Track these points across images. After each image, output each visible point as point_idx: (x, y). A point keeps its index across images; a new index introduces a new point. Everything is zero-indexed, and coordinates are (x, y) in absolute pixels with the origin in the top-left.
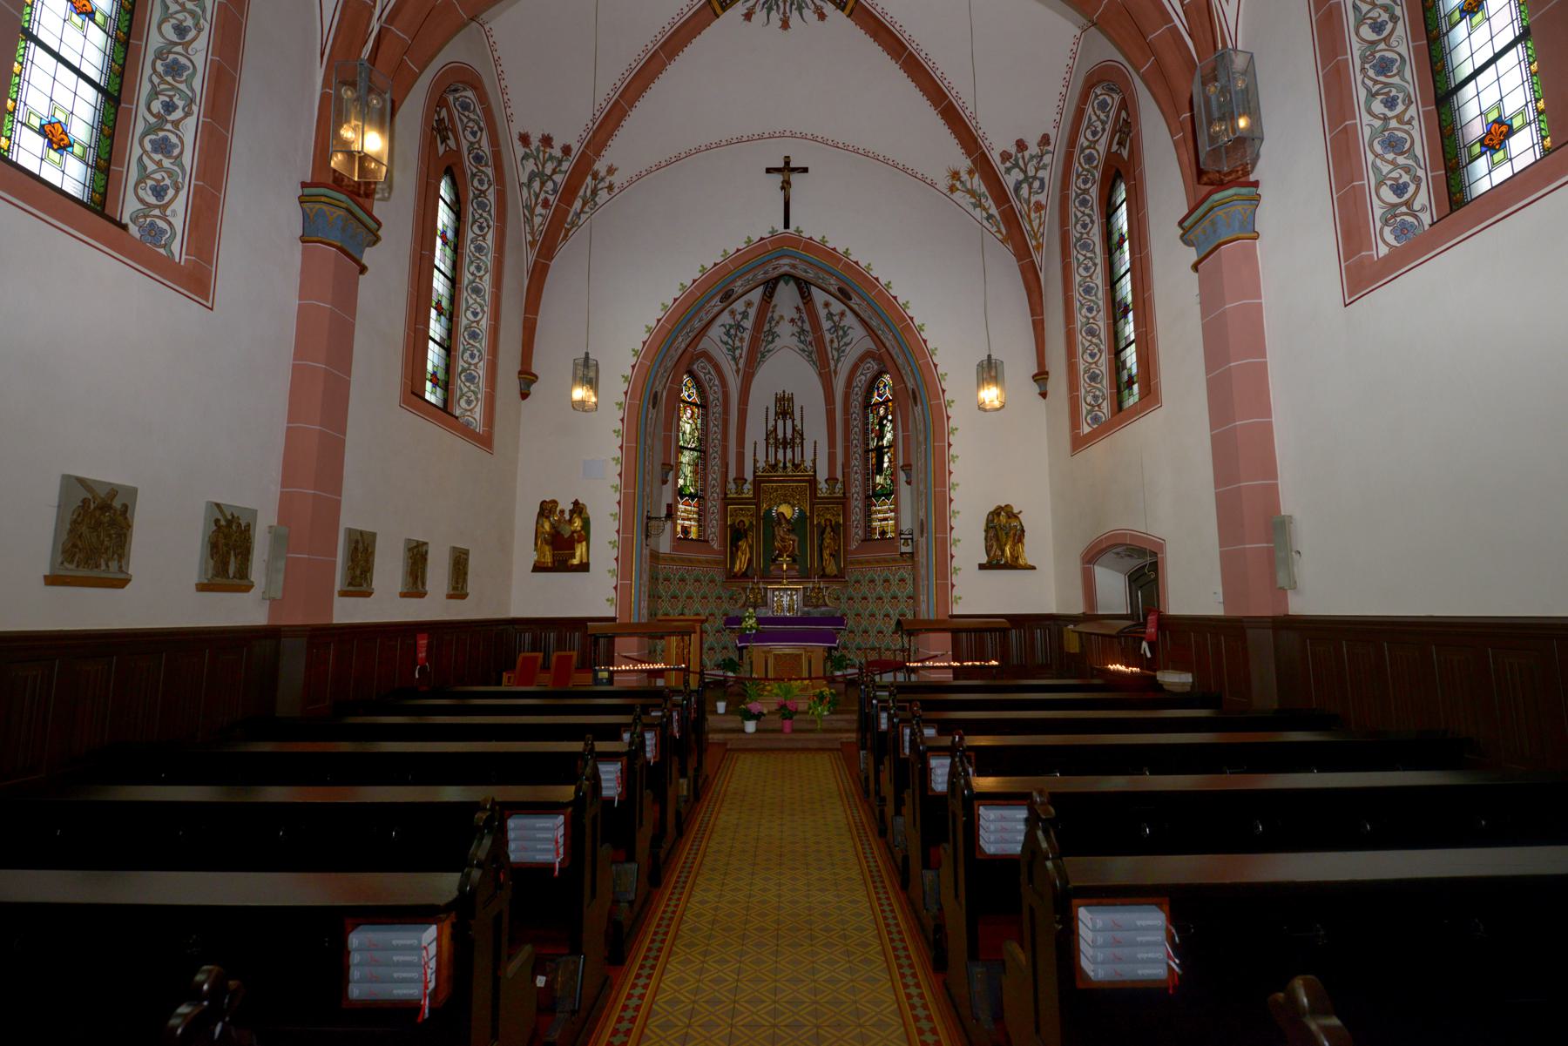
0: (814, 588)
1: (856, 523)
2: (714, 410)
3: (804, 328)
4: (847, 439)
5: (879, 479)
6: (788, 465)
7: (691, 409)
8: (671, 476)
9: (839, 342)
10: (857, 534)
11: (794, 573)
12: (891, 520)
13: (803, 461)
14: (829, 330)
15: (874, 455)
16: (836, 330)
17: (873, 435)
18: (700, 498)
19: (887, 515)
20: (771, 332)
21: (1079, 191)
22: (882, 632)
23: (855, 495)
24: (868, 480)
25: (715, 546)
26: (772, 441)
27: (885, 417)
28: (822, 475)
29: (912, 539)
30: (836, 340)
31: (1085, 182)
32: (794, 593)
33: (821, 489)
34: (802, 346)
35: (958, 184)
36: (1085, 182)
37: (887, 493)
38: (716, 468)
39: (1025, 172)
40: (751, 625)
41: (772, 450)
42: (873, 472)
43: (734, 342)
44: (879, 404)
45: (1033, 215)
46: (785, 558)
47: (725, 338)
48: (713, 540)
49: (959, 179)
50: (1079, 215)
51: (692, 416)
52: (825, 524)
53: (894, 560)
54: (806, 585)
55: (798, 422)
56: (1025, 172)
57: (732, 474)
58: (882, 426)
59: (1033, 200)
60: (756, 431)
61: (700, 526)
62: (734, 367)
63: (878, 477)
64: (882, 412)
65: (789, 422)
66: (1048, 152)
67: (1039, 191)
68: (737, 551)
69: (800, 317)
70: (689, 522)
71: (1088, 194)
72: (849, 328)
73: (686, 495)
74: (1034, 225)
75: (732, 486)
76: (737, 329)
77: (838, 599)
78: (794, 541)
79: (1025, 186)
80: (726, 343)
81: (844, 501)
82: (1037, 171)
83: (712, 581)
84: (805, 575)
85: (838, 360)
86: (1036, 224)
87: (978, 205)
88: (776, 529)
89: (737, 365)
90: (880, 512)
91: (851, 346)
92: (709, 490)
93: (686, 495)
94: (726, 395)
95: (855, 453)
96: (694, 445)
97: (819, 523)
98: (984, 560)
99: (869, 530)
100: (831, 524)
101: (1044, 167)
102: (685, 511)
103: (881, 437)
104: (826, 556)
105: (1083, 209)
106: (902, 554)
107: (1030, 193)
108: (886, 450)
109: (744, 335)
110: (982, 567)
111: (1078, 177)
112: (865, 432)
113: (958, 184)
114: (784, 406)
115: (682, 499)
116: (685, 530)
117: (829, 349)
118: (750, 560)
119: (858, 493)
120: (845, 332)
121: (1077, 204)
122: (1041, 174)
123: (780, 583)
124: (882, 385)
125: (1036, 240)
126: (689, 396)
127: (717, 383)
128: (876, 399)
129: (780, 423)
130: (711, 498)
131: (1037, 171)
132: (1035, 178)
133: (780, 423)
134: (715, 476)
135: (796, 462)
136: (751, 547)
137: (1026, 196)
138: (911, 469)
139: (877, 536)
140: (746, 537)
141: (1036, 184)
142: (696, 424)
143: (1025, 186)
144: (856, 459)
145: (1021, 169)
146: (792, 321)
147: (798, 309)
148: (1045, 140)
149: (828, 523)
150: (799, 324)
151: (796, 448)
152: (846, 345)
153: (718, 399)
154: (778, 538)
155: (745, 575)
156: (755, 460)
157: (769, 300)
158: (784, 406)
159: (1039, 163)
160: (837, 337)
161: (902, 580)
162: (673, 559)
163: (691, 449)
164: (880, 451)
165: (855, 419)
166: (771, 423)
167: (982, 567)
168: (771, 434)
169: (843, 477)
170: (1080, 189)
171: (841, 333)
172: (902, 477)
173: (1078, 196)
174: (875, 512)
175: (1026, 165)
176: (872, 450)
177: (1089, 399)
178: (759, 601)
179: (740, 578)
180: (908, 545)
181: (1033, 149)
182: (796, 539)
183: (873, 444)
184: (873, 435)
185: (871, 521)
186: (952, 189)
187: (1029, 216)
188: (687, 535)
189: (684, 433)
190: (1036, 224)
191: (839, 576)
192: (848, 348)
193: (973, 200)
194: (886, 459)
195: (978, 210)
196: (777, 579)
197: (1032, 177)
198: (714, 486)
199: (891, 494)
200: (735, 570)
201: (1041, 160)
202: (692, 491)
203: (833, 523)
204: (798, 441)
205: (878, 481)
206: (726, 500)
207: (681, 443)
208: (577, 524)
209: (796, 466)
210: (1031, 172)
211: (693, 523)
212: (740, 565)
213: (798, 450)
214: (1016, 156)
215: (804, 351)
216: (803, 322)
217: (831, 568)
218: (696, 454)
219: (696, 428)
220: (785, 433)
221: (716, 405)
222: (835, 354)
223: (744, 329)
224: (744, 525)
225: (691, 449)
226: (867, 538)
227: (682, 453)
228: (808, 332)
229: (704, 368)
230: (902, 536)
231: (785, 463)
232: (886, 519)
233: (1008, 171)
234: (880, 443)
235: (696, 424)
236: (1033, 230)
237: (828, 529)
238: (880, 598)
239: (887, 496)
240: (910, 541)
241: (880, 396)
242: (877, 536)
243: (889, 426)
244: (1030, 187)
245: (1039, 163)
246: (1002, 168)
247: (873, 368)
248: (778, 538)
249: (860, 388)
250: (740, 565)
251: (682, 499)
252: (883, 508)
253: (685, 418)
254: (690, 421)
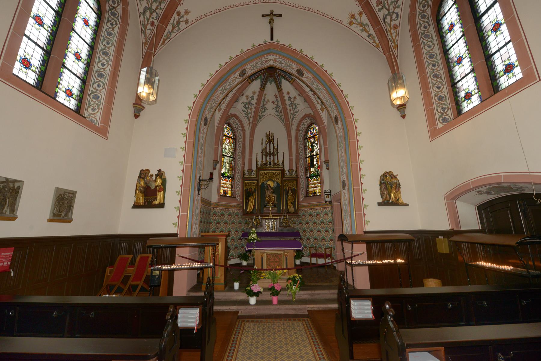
0: (284, 219)
1: (302, 189)
2: (239, 139)
3: (278, 105)
4: (297, 152)
5: (312, 169)
6: (272, 163)
7: (229, 139)
8: (218, 166)
9: (293, 111)
10: (302, 194)
11: (274, 211)
12: (318, 187)
13: (278, 161)
14: (289, 105)
15: (309, 159)
16: (292, 105)
17: (309, 151)
18: (232, 178)
19: (316, 185)
20: (263, 107)
21: (421, 12)
22: (317, 239)
23: (301, 177)
24: (307, 170)
25: (239, 200)
26: (264, 153)
27: (314, 143)
28: (287, 168)
29: (330, 194)
30: (292, 110)
31: (424, 7)
32: (275, 221)
33: (286, 174)
34: (277, 114)
35: (354, 21)
36: (424, 7)
37: (316, 175)
38: (240, 165)
39: (388, 10)
40: (254, 238)
41: (264, 157)
42: (309, 167)
43: (248, 111)
44: (311, 137)
45: (392, 31)
46: (271, 204)
47: (244, 109)
48: (238, 197)
49: (354, 18)
51: (229, 142)
52: (289, 189)
53: (322, 205)
54: (280, 217)
55: (276, 145)
56: (388, 10)
57: (247, 168)
58: (313, 146)
59: (393, 23)
60: (257, 149)
61: (232, 191)
62: (248, 122)
63: (311, 168)
64: (312, 140)
65: (272, 145)
67: (396, 19)
68: (249, 202)
69: (277, 99)
70: (227, 189)
71: (426, 12)
72: (298, 104)
73: (226, 177)
74: (393, 36)
75: (246, 172)
76: (249, 104)
77: (295, 223)
78: (274, 197)
79: (388, 17)
80: (244, 111)
81: (296, 179)
82: (394, 9)
83: (237, 215)
84: (279, 213)
85: (293, 119)
86: (394, 35)
87: (364, 30)
88: (266, 191)
89: (249, 121)
90: (313, 184)
91: (298, 113)
92: (236, 175)
93: (226, 177)
94: (244, 134)
95: (301, 158)
96: (230, 155)
97: (286, 189)
98: (380, 200)
99: (308, 192)
100: (291, 189)
101: (398, 7)
102: (225, 184)
103: (312, 151)
104: (289, 204)
105: (423, 20)
106: (326, 202)
107: (391, 21)
108: (315, 156)
109: (252, 107)
110: (379, 204)
111: (420, 4)
112: (305, 150)
113: (354, 21)
114: (270, 139)
115: (224, 178)
116: (225, 192)
117: (289, 113)
118: (255, 206)
119: (303, 176)
120: (296, 106)
121: (420, 18)
122: (396, 10)
123: (268, 216)
124: (312, 129)
125: (394, 43)
126: (228, 134)
127: (240, 128)
128: (309, 135)
129: (268, 145)
130: (237, 178)
131: (394, 9)
132: (393, 12)
133: (268, 145)
134: (239, 169)
135: (275, 162)
136: (255, 200)
137: (389, 22)
138: (329, 162)
139: (312, 195)
140: (253, 196)
141: (394, 16)
142: (231, 146)
143: (388, 17)
144: (301, 161)
145: (386, 9)
146: (273, 102)
147: (276, 96)
149: (290, 189)
150: (276, 103)
151: (275, 156)
152: (296, 112)
153: (241, 136)
154: (267, 195)
155: (252, 213)
156: (257, 161)
157: (263, 90)
158: (270, 139)
159: (395, 5)
160: (293, 108)
161: (326, 214)
162: (218, 205)
163: (228, 156)
164: (312, 157)
165: (301, 144)
166: (264, 145)
167: (379, 204)
168: (264, 151)
169: (296, 168)
170: (421, 10)
171: (294, 107)
172: (324, 166)
173: (420, 14)
174: (311, 184)
175: (389, 7)
176: (308, 157)
178: (259, 224)
179: (249, 214)
180: (329, 197)
182: (275, 196)
183: (309, 155)
184: (309, 151)
185: (308, 188)
186: (351, 23)
187: (390, 32)
188: (226, 194)
189: (225, 149)
191: (296, 214)
192: (297, 114)
193: (361, 28)
194: (315, 160)
195: (364, 32)
196: (267, 215)
197: (392, 12)
198: (238, 173)
199: (318, 176)
200: (248, 210)
201: (397, 3)
202: (229, 175)
203: (292, 189)
204: (276, 153)
205: (311, 170)
206: (244, 179)
207: (224, 153)
208: (159, 181)
209: (275, 164)
210: (391, 10)
211: (229, 189)
212: (250, 208)
213: (276, 157)
214: (384, 2)
215: (278, 116)
216: (278, 102)
217: (292, 209)
218: (231, 159)
219: (231, 148)
220: (270, 150)
221: (240, 138)
222: (292, 116)
223: (252, 104)
224: (252, 190)
225: (228, 156)
226: (307, 196)
227: (224, 158)
228: (280, 106)
229: (235, 122)
230: (326, 193)
231: (270, 162)
232: (316, 187)
233: (380, 10)
234: (312, 154)
235: (231, 146)
236: (393, 38)
237: (290, 191)
238: (315, 223)
239: (316, 176)
240: (329, 196)
241: (311, 134)
242: (312, 195)
243: (316, 146)
244: (391, 17)
245: (395, 5)
246: (377, 9)
247: (308, 122)
248: (267, 195)
249: (302, 131)
250: (250, 208)
251: (224, 178)
252: (314, 182)
253: (226, 143)
254: (228, 144)
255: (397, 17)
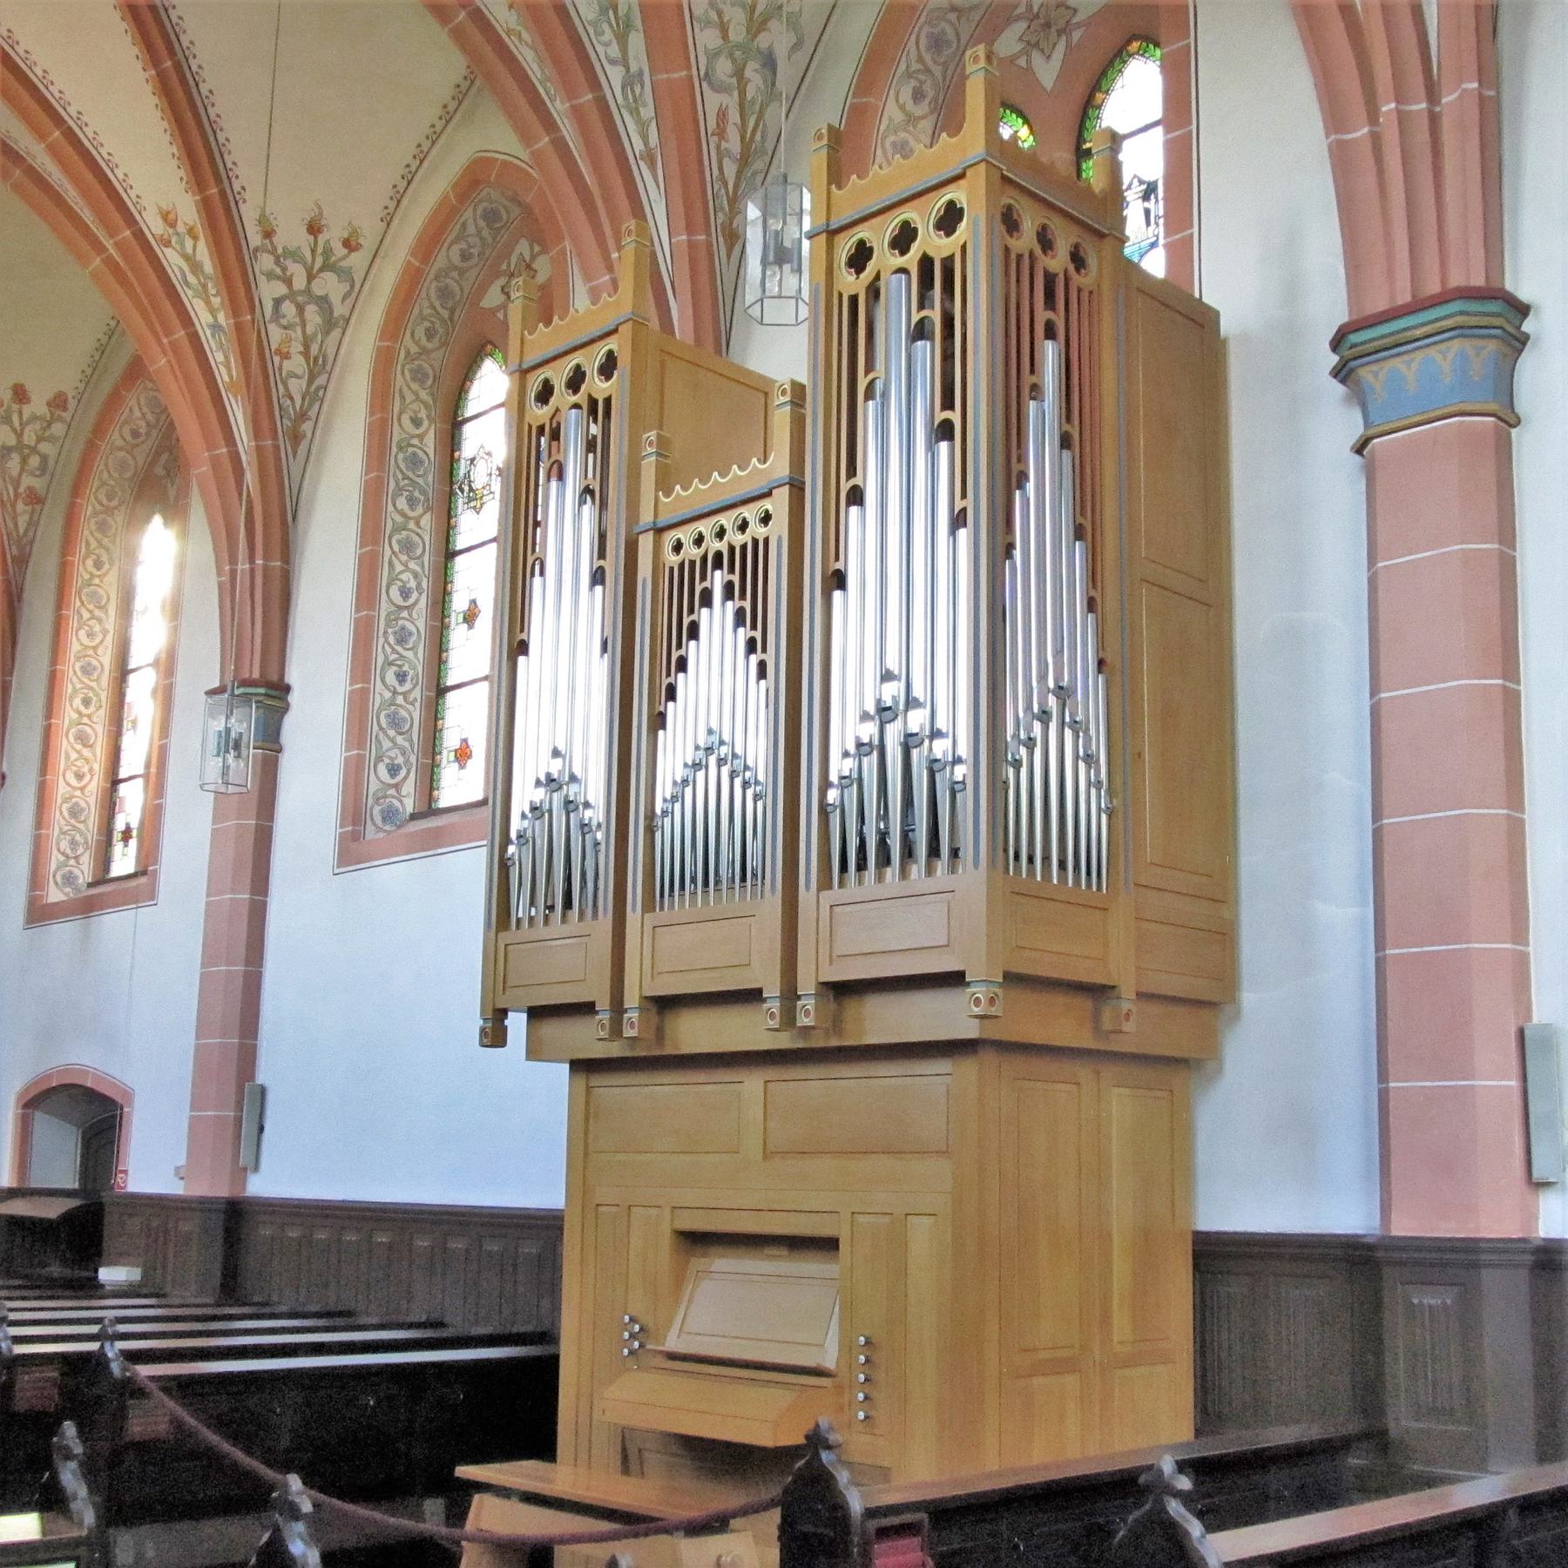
21: (99, 508)
39: (19, 435)
45: (20, 506)
50: (94, 544)
56: (19, 435)
59: (27, 481)
66: (60, 419)
67: (38, 473)
74: (20, 524)
79: (16, 457)
82: (40, 440)
86: (22, 522)
101: (51, 439)
107: (22, 470)
122: (44, 447)
132: (34, 450)
137: (15, 473)
143: (16, 457)
145: (14, 430)
148: (59, 402)
170: (101, 504)
173: (96, 514)
177: (64, 845)
181: (38, 405)
187: (13, 506)
190: (22, 522)
201: (49, 426)
214: (9, 407)
236: (16, 525)
244: (24, 461)
245: (44, 429)
255: (43, 468)
